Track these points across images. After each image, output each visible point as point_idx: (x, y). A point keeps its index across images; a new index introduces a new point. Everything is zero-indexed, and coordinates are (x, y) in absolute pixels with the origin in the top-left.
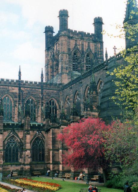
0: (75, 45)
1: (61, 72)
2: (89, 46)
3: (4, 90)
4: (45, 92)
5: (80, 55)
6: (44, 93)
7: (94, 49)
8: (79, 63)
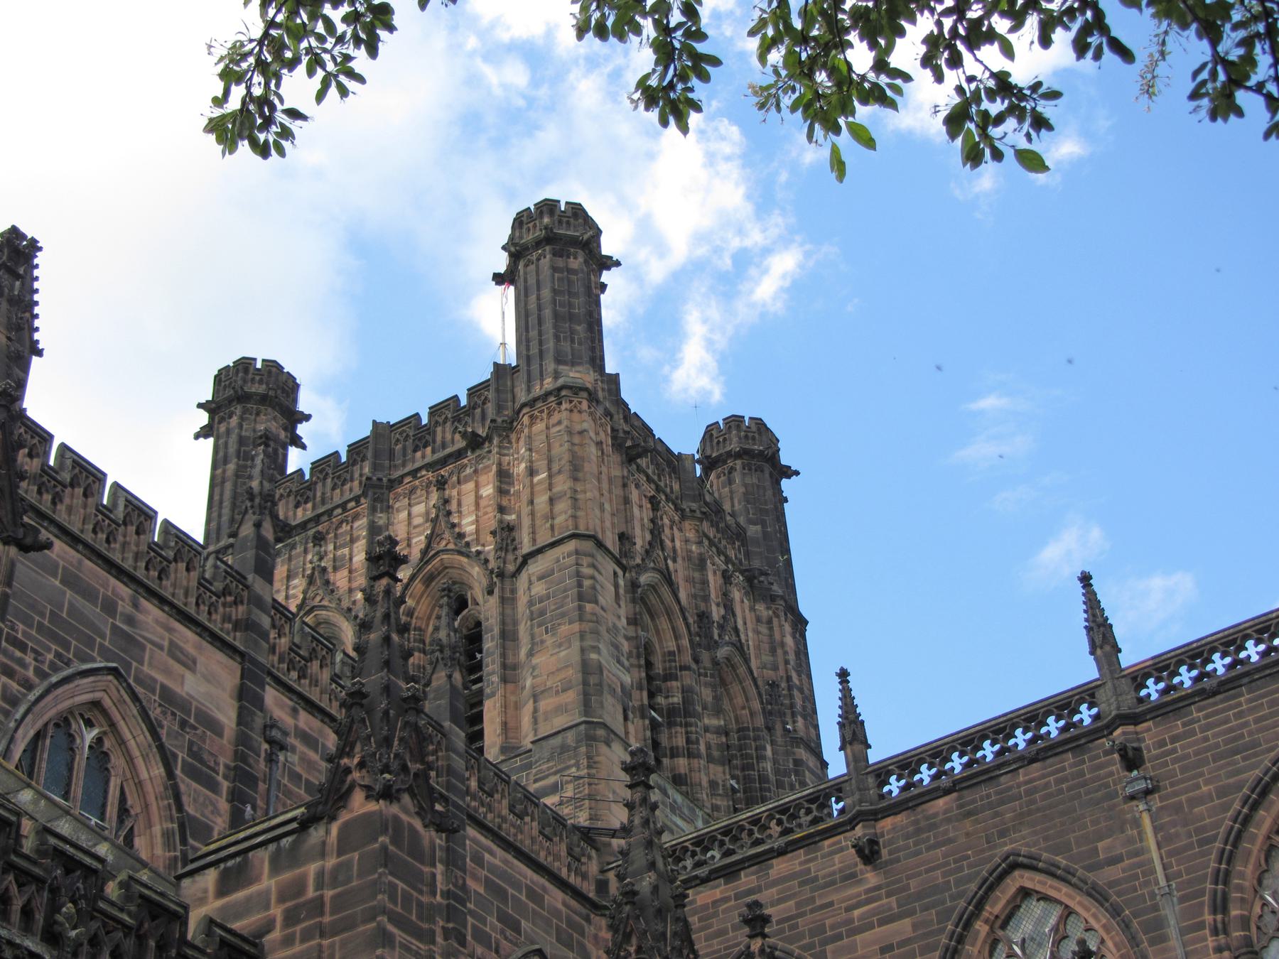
0: (648, 537)
1: (586, 713)
2: (728, 606)
3: (80, 602)
4: (478, 860)
5: (685, 642)
6: (475, 878)
7: (758, 648)
8: (671, 713)
